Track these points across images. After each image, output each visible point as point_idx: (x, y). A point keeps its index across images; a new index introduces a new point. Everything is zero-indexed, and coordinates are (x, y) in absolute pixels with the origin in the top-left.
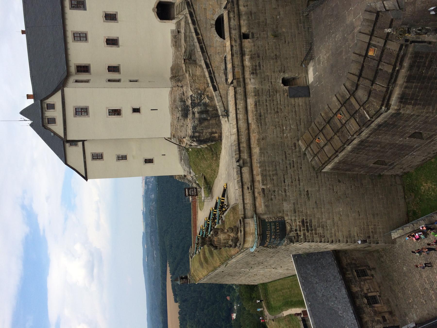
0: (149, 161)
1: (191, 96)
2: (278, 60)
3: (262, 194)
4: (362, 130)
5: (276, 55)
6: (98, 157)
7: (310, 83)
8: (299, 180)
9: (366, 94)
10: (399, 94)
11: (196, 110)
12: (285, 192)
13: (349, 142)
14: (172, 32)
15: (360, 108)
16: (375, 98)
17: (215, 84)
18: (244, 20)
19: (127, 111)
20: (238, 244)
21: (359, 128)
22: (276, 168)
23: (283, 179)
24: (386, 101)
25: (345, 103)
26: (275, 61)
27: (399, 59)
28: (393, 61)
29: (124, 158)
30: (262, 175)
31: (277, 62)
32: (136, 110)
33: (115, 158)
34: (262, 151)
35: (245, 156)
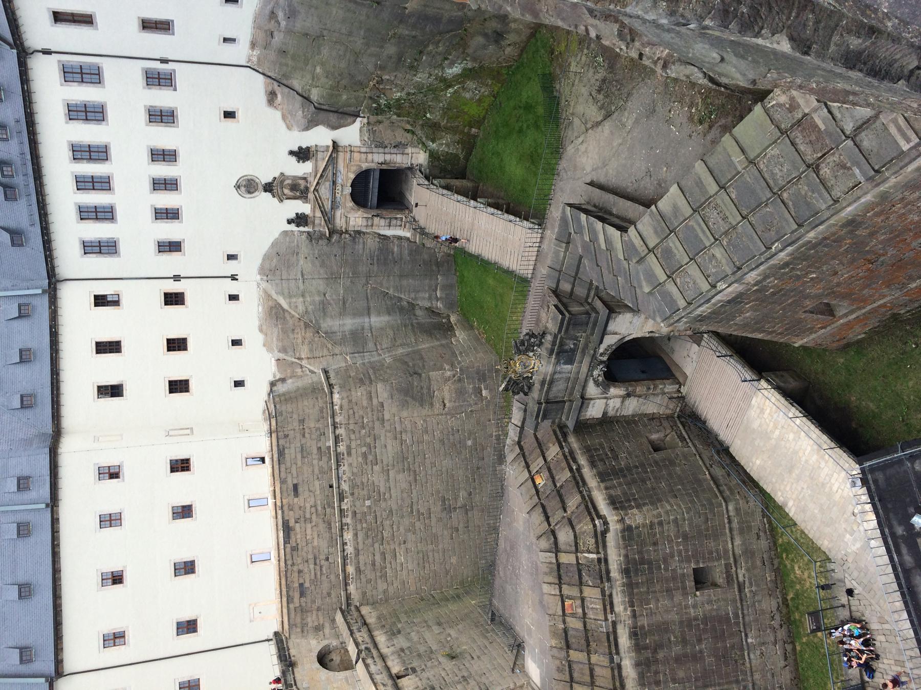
2: (470, 681)
4: (607, 593)
5: (463, 677)
7: (539, 685)
9: (568, 529)
10: (605, 499)
13: (612, 638)
15: (577, 558)
16: (580, 522)
18: (393, 660)
21: (599, 589)
24: (592, 510)
25: (560, 578)
26: (464, 683)
27: (570, 457)
28: (564, 464)
31: (468, 683)
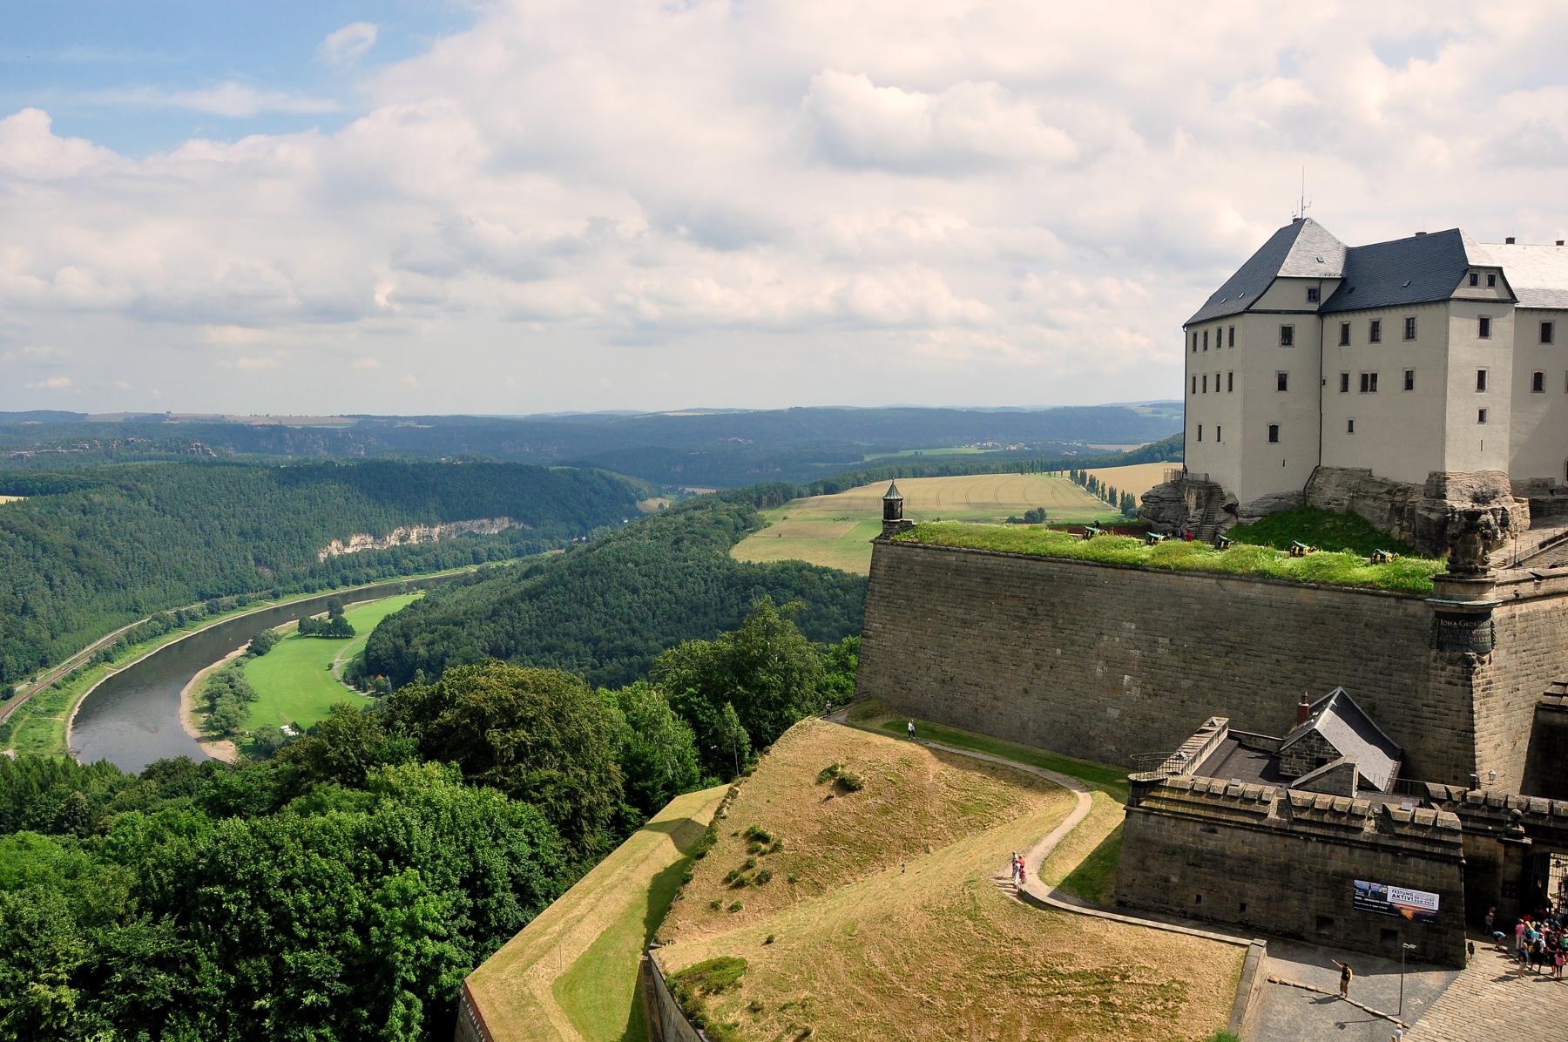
0: (1274, 433)
1: (1504, 509)
3: (1510, 614)
6: (1287, 335)
8: (1527, 675)
11: (1491, 517)
12: (1516, 652)
14: (1552, 480)
17: (1548, 547)
19: (1482, 400)
20: (1461, 574)
22: (1537, 636)
23: (1525, 648)
29: (1282, 385)
30: (1528, 614)
32: (1482, 416)
33: (1283, 369)
34: (1548, 613)
35: (1545, 587)
